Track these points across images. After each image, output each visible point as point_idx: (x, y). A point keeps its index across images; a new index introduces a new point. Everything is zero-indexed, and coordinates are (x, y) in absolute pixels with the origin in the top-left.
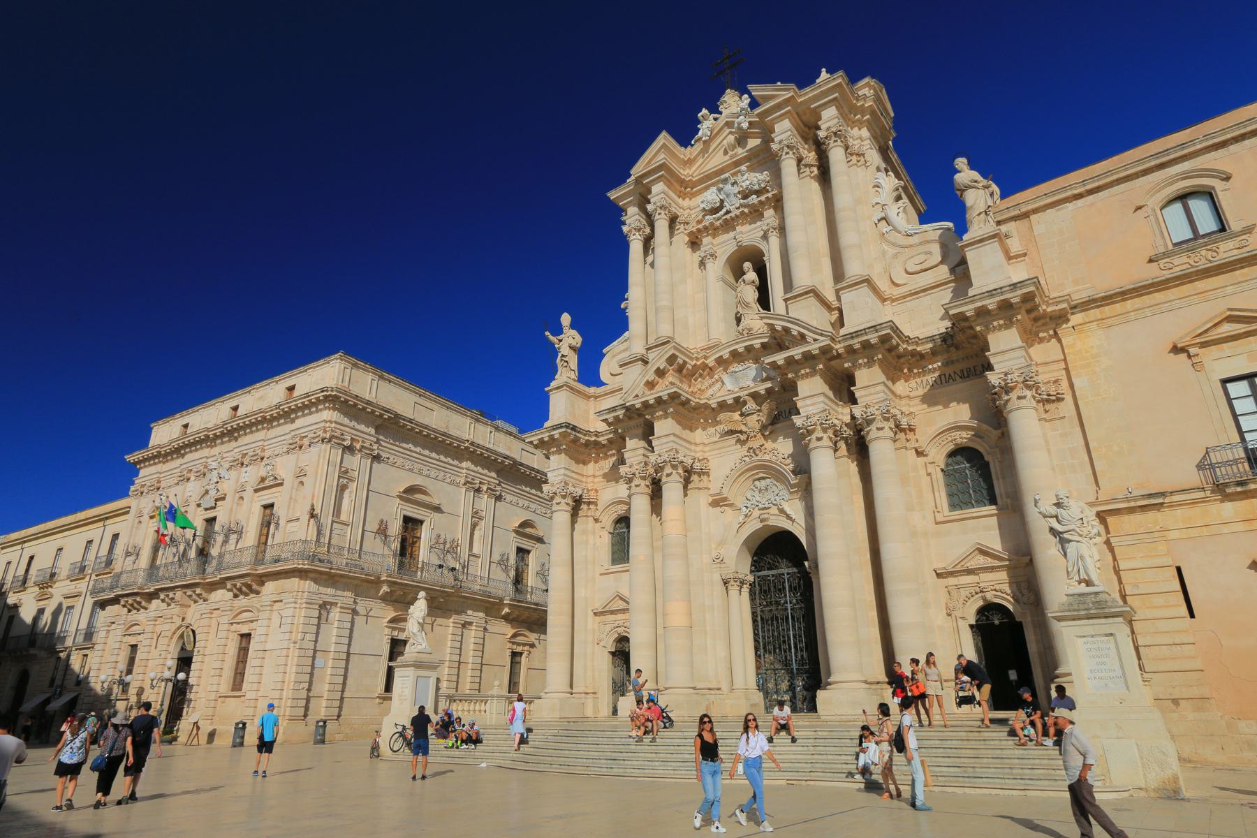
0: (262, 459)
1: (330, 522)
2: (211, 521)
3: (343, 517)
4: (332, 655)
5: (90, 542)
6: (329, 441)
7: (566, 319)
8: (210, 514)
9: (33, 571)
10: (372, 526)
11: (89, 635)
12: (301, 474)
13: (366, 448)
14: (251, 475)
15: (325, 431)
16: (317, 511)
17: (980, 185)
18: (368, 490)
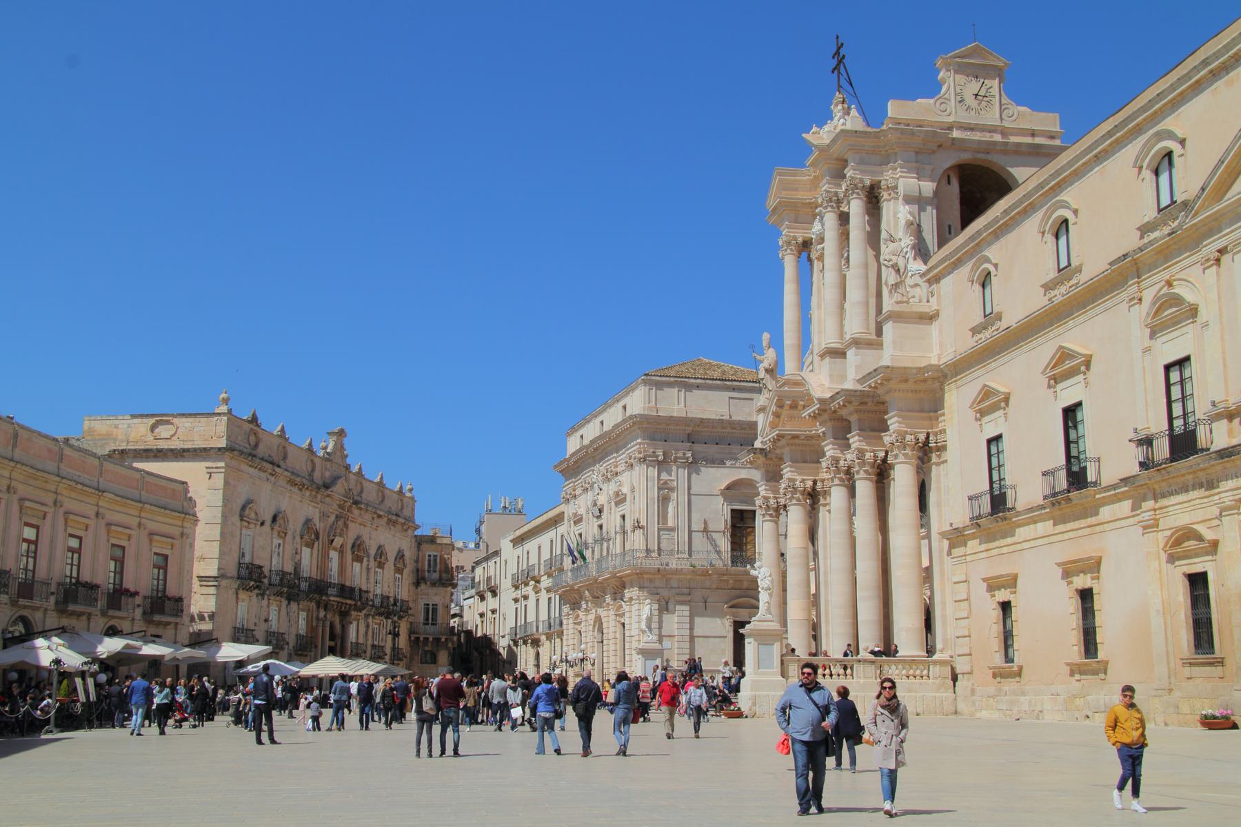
0: (617, 473)
1: (656, 529)
2: (601, 527)
3: (670, 523)
4: (676, 639)
5: (552, 541)
6: (644, 461)
7: (766, 337)
8: (599, 523)
9: (542, 562)
10: (697, 525)
11: (561, 624)
12: (633, 490)
13: (680, 458)
14: (611, 488)
15: (640, 453)
16: (643, 523)
17: (891, 263)
18: (689, 494)
